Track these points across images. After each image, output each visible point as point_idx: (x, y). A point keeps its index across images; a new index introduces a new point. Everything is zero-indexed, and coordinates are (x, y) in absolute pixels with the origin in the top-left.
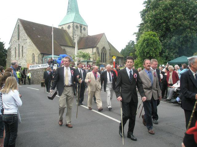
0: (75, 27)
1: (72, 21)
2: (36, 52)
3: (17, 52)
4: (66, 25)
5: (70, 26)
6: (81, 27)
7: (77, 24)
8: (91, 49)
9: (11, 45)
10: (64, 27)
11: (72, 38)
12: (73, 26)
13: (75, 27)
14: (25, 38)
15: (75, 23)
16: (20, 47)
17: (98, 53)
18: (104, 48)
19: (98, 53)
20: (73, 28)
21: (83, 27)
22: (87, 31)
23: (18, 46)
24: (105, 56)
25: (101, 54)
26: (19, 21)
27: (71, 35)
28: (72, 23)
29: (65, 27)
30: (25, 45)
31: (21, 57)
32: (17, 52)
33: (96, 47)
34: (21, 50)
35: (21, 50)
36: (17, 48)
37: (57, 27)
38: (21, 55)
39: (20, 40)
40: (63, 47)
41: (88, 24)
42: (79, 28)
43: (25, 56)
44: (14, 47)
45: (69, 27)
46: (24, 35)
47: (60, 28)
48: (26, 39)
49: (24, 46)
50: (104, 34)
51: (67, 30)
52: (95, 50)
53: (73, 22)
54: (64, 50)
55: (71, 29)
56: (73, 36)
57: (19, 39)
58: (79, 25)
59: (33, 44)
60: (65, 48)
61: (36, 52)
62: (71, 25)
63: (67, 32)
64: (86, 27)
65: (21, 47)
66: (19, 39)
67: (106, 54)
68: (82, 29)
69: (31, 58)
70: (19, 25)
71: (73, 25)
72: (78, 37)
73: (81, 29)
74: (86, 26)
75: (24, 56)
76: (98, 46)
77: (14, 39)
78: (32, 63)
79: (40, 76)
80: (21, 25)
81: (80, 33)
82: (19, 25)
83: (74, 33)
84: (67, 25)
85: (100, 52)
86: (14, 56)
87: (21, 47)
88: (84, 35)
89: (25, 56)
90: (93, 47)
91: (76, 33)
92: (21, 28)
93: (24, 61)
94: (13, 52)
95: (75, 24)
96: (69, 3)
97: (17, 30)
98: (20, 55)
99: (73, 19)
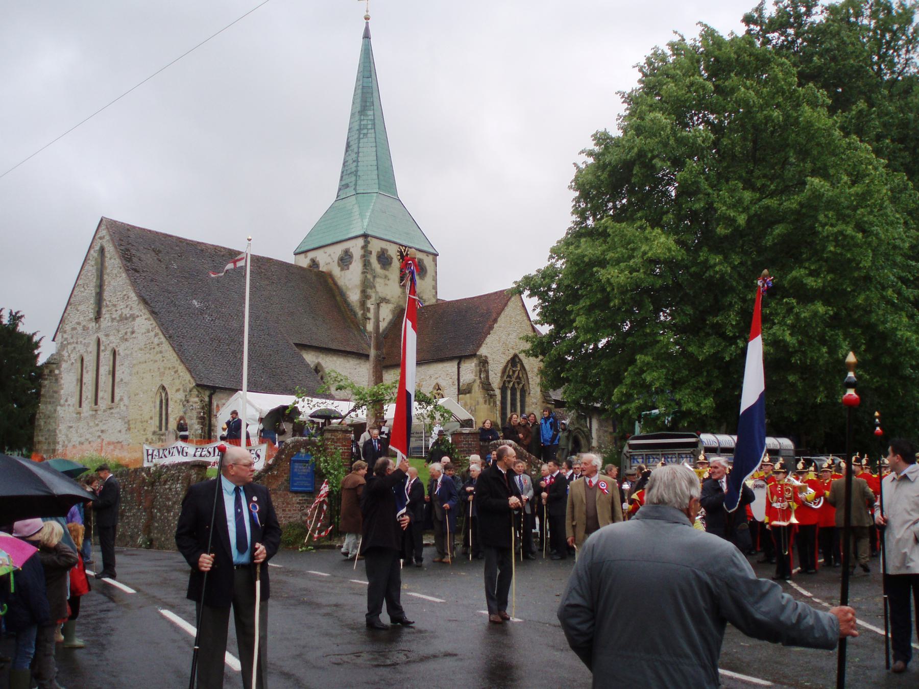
0: (373, 260)
1: (362, 232)
2: (177, 382)
3: (89, 378)
4: (329, 250)
5: (351, 257)
7: (384, 245)
8: (450, 368)
9: (63, 347)
10: (320, 256)
12: (366, 253)
13: (373, 260)
14: (127, 312)
16: (102, 354)
17: (486, 386)
18: (514, 361)
19: (486, 386)
20: (366, 264)
22: (435, 280)
23: (93, 348)
24: (519, 404)
25: (498, 392)
26: (103, 232)
27: (354, 297)
28: (360, 242)
29: (327, 260)
30: (128, 344)
31: (104, 403)
32: (89, 378)
33: (473, 355)
34: (104, 369)
35: (104, 369)
36: (86, 360)
37: (290, 259)
38: (104, 394)
39: (105, 322)
40: (310, 358)
43: (121, 400)
44: (75, 356)
45: (345, 260)
46: (126, 298)
47: (304, 262)
48: (134, 317)
49: (121, 350)
51: (336, 271)
52: (469, 371)
53: (365, 236)
54: (317, 369)
55: (356, 266)
56: (363, 304)
57: (98, 317)
58: (393, 251)
59: (163, 339)
61: (177, 382)
62: (356, 248)
63: (335, 284)
65: (106, 357)
66: (98, 317)
67: (524, 392)
69: (150, 409)
70: (102, 250)
71: (365, 247)
72: (391, 306)
75: (117, 399)
76: (483, 351)
77: (74, 318)
78: (154, 433)
79: (174, 503)
80: (110, 249)
82: (102, 250)
83: (366, 287)
84: (338, 250)
85: (496, 381)
86: (74, 400)
87: (106, 357)
89: (121, 400)
90: (460, 359)
91: (379, 284)
92: (113, 262)
93: (120, 425)
94: (68, 380)
95: (375, 247)
96: (348, 146)
97: (91, 269)
98: (100, 394)
99: (366, 224)
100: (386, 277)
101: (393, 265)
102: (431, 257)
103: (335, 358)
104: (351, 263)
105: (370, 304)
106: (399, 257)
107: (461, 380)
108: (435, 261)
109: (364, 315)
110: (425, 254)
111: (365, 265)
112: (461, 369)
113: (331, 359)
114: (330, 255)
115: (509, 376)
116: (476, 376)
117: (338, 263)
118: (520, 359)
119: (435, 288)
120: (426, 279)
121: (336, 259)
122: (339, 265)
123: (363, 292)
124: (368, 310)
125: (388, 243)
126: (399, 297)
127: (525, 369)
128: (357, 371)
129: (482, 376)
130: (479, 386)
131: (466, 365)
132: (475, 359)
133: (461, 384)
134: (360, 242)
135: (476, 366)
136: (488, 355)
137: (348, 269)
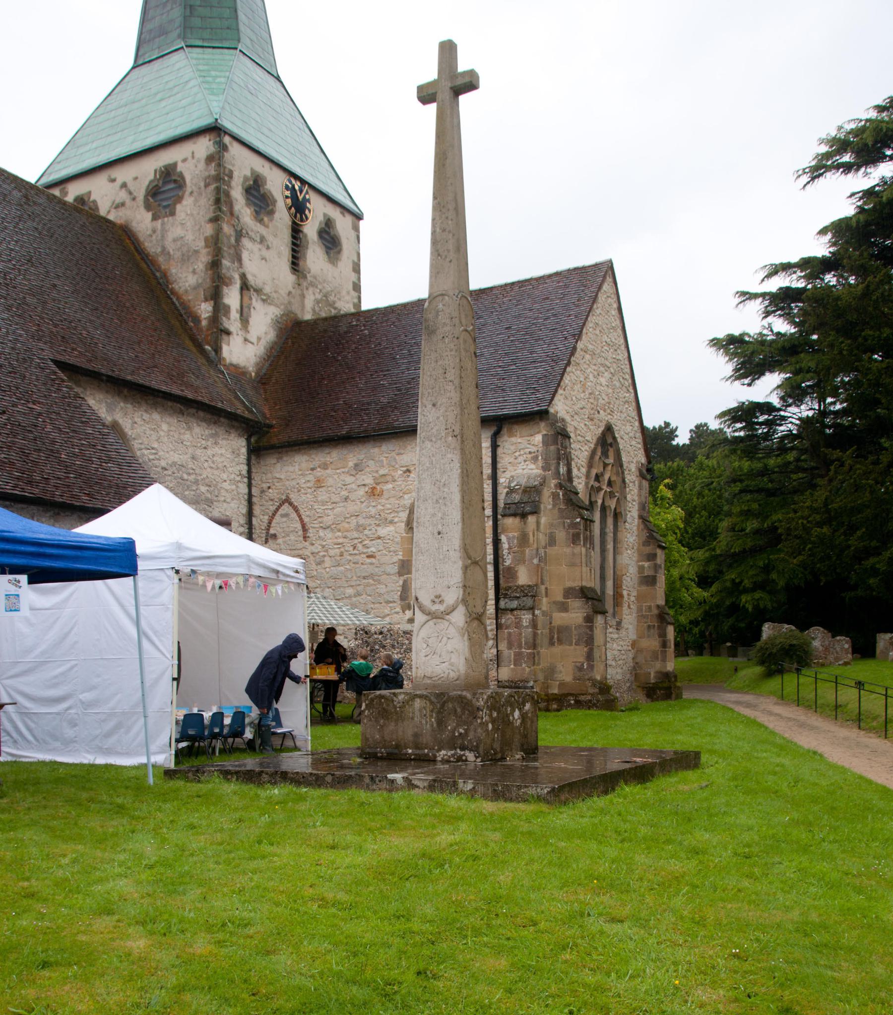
0: (237, 194)
4: (123, 174)
6: (299, 208)
11: (205, 310)
13: (237, 194)
15: (235, 150)
21: (317, 209)
22: (357, 269)
28: (204, 146)
33: (542, 415)
41: (363, 204)
42: (282, 216)
50: (606, 270)
58: (275, 184)
60: (126, 424)
64: (342, 224)
67: (617, 515)
68: (310, 229)
71: (216, 158)
73: (296, 231)
74: (344, 209)
81: (287, 278)
84: (148, 169)
88: (325, 299)
100: (262, 240)
101: (277, 215)
102: (349, 219)
103: (156, 416)
104: (179, 199)
105: (232, 298)
106: (289, 201)
107: (502, 480)
108: (356, 229)
109: (215, 319)
110: (338, 210)
111: (217, 201)
112: (500, 451)
113: (146, 416)
114: (124, 185)
115: (598, 478)
116: (544, 469)
117: (146, 197)
118: (614, 438)
119: (357, 287)
120: (341, 264)
121: (141, 195)
122: (148, 207)
123: (215, 265)
124: (227, 309)
125: (267, 165)
126: (290, 293)
127: (621, 466)
128: (209, 452)
129: (561, 470)
130: (555, 496)
131: (513, 439)
132: (543, 424)
133: (502, 492)
134: (204, 146)
135: (545, 443)
136: (568, 418)
137: (173, 214)
